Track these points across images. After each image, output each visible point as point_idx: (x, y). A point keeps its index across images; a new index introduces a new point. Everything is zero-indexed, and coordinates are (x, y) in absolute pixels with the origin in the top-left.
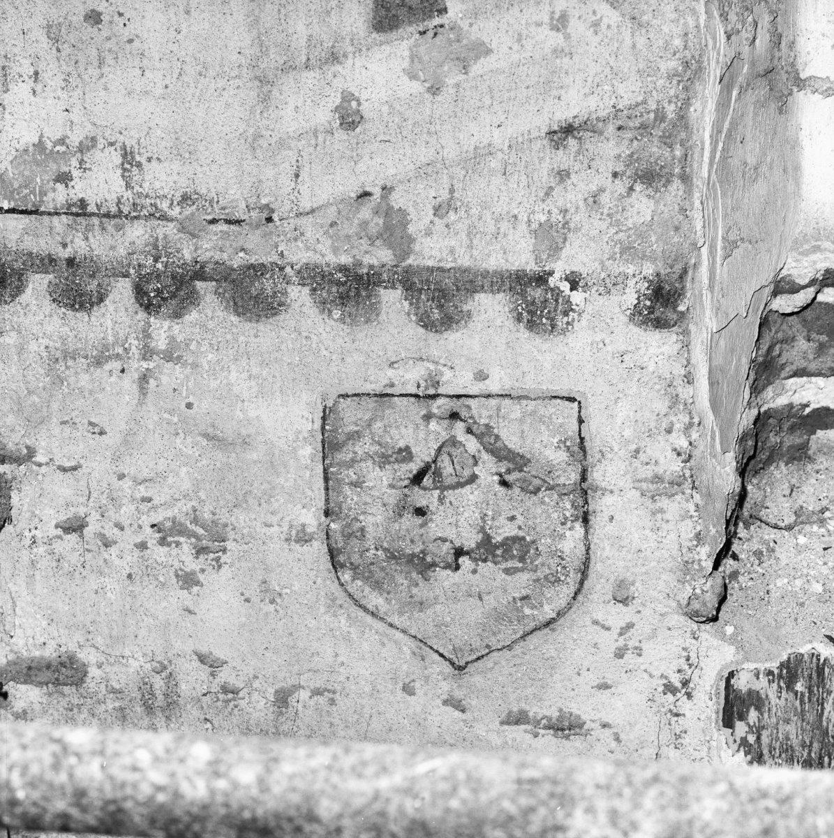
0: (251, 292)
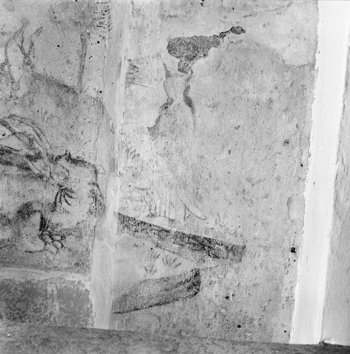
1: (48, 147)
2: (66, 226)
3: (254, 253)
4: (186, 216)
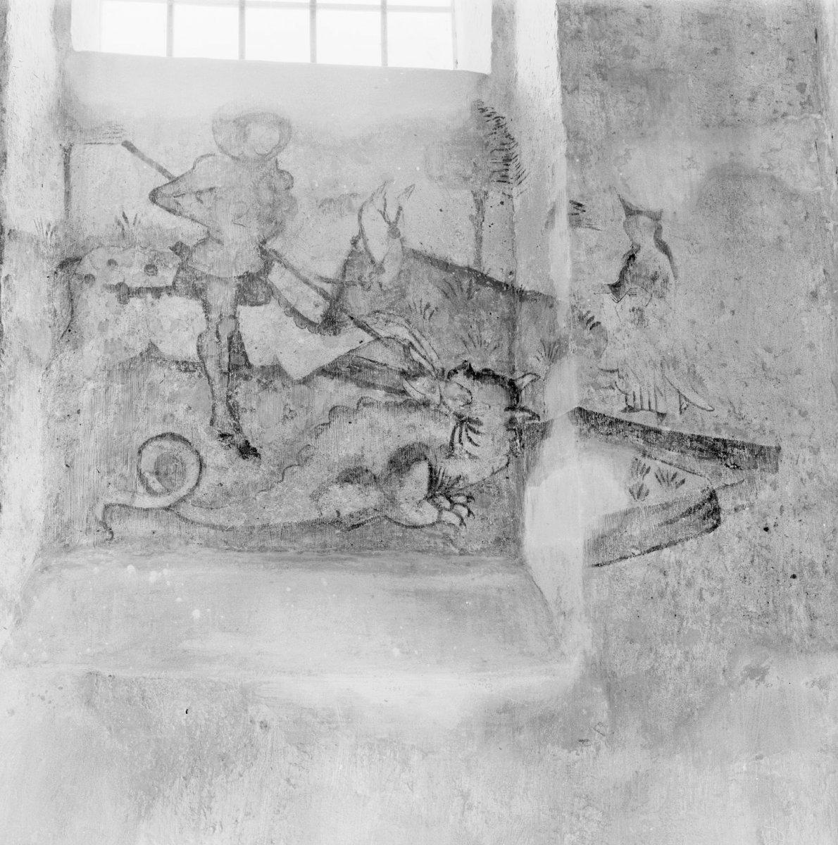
2: (473, 479)
3: (795, 457)
4: (683, 407)
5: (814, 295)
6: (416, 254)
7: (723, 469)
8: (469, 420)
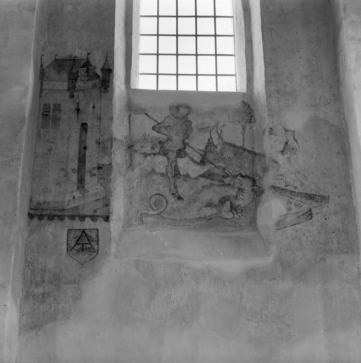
0: (61, 218)
1: (232, 172)
2: (243, 205)
3: (334, 199)
5: (338, 153)
6: (226, 143)
7: (313, 202)
8: (242, 189)
